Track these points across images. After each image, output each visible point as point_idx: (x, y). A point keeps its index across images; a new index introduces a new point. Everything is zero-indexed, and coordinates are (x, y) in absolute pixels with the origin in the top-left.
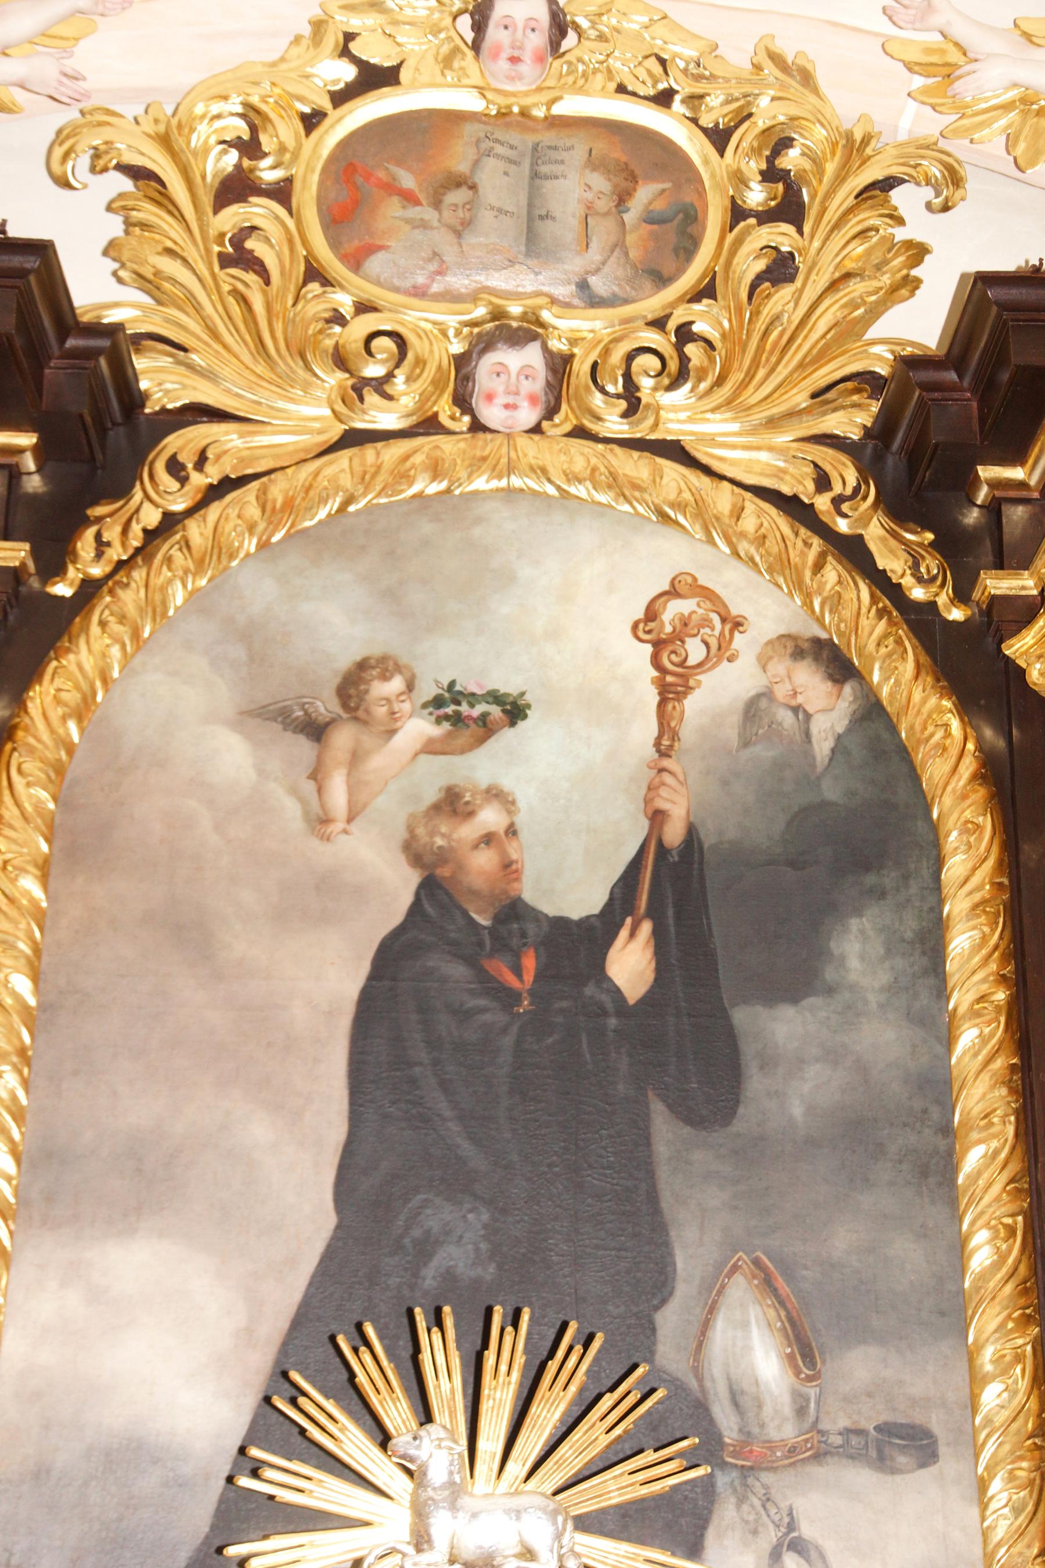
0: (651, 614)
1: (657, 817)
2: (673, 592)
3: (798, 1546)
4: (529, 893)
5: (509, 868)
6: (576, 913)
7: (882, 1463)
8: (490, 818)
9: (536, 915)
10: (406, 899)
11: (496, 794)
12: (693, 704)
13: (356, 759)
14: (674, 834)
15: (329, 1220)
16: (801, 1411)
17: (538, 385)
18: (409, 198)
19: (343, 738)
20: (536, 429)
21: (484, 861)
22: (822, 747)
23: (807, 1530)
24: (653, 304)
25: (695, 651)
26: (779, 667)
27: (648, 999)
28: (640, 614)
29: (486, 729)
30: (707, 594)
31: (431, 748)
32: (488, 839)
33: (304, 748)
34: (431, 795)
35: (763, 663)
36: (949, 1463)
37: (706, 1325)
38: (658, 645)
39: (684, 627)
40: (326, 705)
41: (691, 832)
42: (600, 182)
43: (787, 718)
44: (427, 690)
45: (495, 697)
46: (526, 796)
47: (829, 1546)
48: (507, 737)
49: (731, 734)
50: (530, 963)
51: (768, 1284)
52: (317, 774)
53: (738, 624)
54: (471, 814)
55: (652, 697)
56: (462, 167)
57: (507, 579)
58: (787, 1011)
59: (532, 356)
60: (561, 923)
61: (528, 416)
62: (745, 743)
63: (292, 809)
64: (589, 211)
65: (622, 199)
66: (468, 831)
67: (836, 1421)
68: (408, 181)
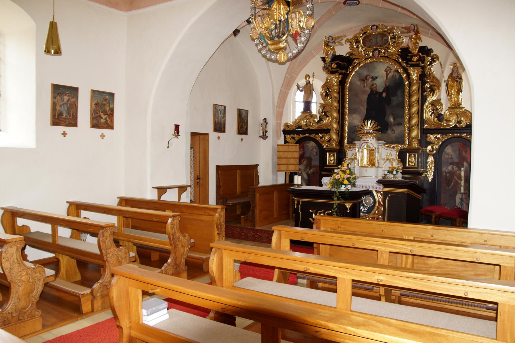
0: (386, 69)
1: (386, 85)
2: (387, 68)
3: (393, 130)
4: (378, 90)
5: (376, 89)
6: (381, 92)
7: (399, 125)
8: (375, 85)
9: (378, 92)
10: (370, 92)
11: (376, 84)
12: (388, 76)
13: (367, 82)
14: (387, 86)
15: (366, 113)
16: (394, 122)
17: (378, 53)
18: (368, 41)
19: (366, 81)
20: (378, 56)
21: (375, 89)
22: (397, 78)
23: (394, 129)
24: (386, 46)
25: (389, 72)
26: (394, 73)
27: (386, 97)
28: (385, 69)
29: (375, 79)
30: (390, 68)
31: (371, 81)
32: (375, 87)
33: (363, 82)
34: (371, 84)
35: (393, 72)
36: (403, 125)
37: (388, 118)
38: (386, 72)
39: (388, 70)
40: (364, 79)
41: (388, 85)
42: (381, 38)
43: (395, 76)
44: (371, 77)
45: (375, 77)
46: (377, 84)
47: (395, 130)
48: (376, 80)
49: (391, 78)
50: (378, 96)
51: (392, 115)
52: (364, 84)
53: (391, 70)
54: (374, 85)
55: (386, 76)
56: (371, 38)
57: (376, 68)
58: (394, 97)
59: (377, 51)
60: (380, 92)
61: (377, 56)
62: (392, 78)
63: (363, 86)
64: (380, 40)
65: (382, 39)
66: (374, 87)
67: (396, 123)
68: (368, 40)
